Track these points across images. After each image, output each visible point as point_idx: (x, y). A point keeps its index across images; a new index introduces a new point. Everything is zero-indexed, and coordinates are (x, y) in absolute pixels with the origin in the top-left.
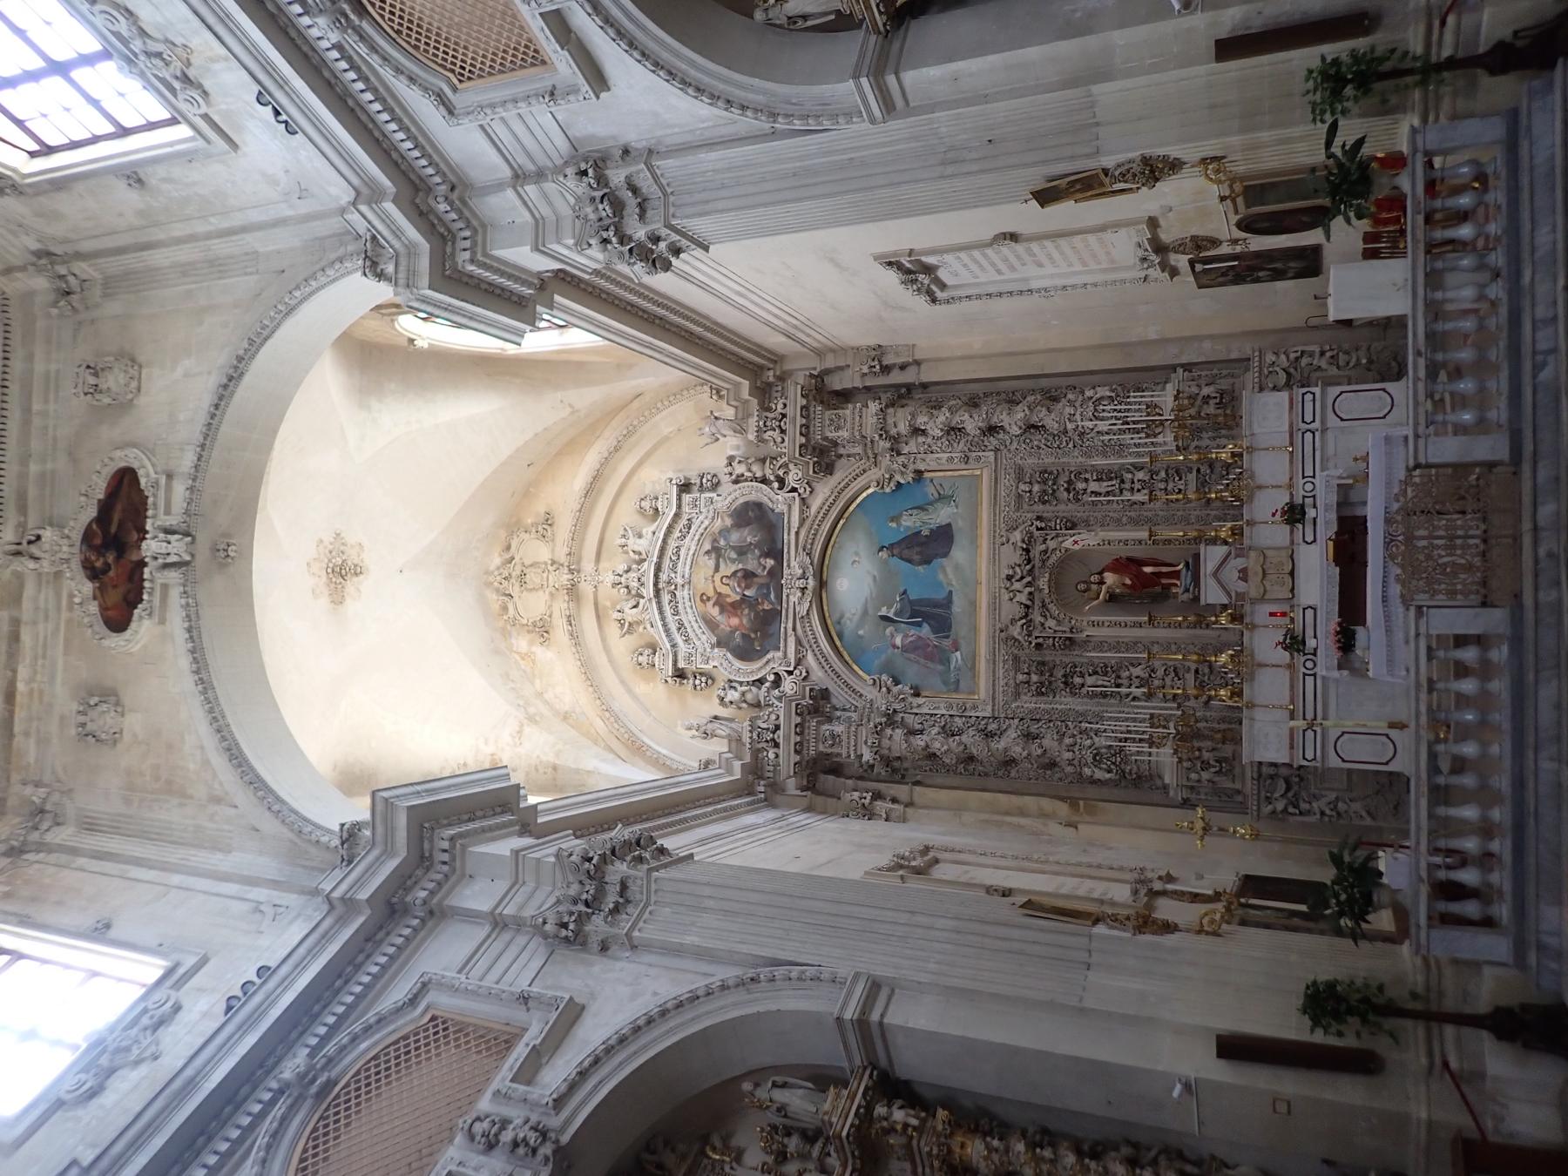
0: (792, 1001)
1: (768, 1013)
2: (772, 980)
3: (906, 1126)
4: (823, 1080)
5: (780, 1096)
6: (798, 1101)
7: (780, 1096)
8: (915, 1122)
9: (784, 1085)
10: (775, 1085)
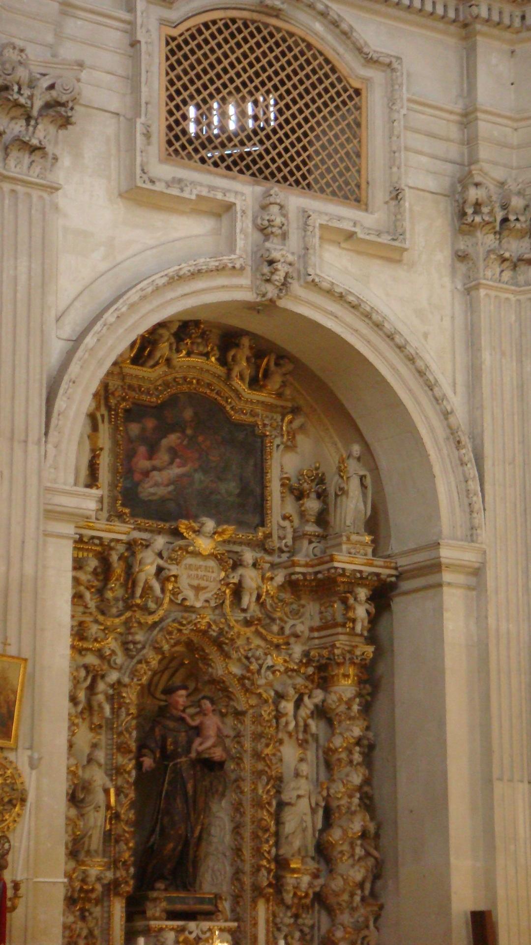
0: (445, 488)
1: (430, 467)
2: (463, 464)
3: (354, 621)
4: (374, 524)
5: (354, 486)
6: (352, 507)
7: (354, 486)
8: (358, 628)
9: (363, 486)
10: (362, 478)
